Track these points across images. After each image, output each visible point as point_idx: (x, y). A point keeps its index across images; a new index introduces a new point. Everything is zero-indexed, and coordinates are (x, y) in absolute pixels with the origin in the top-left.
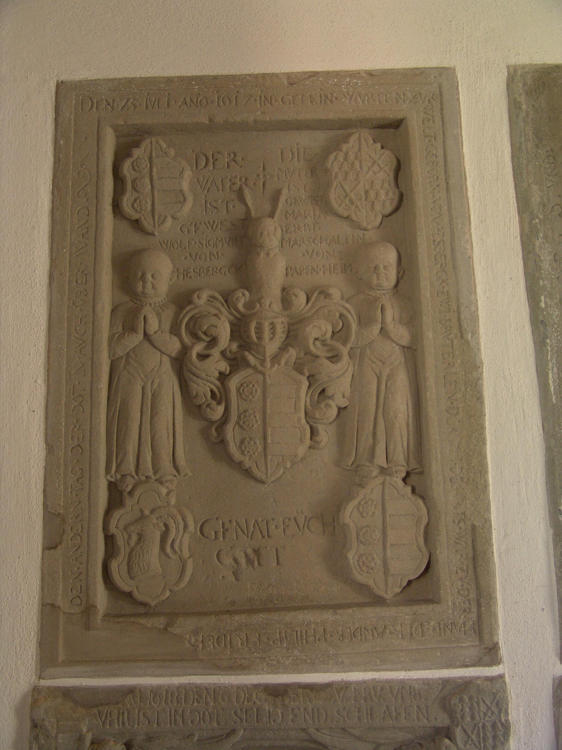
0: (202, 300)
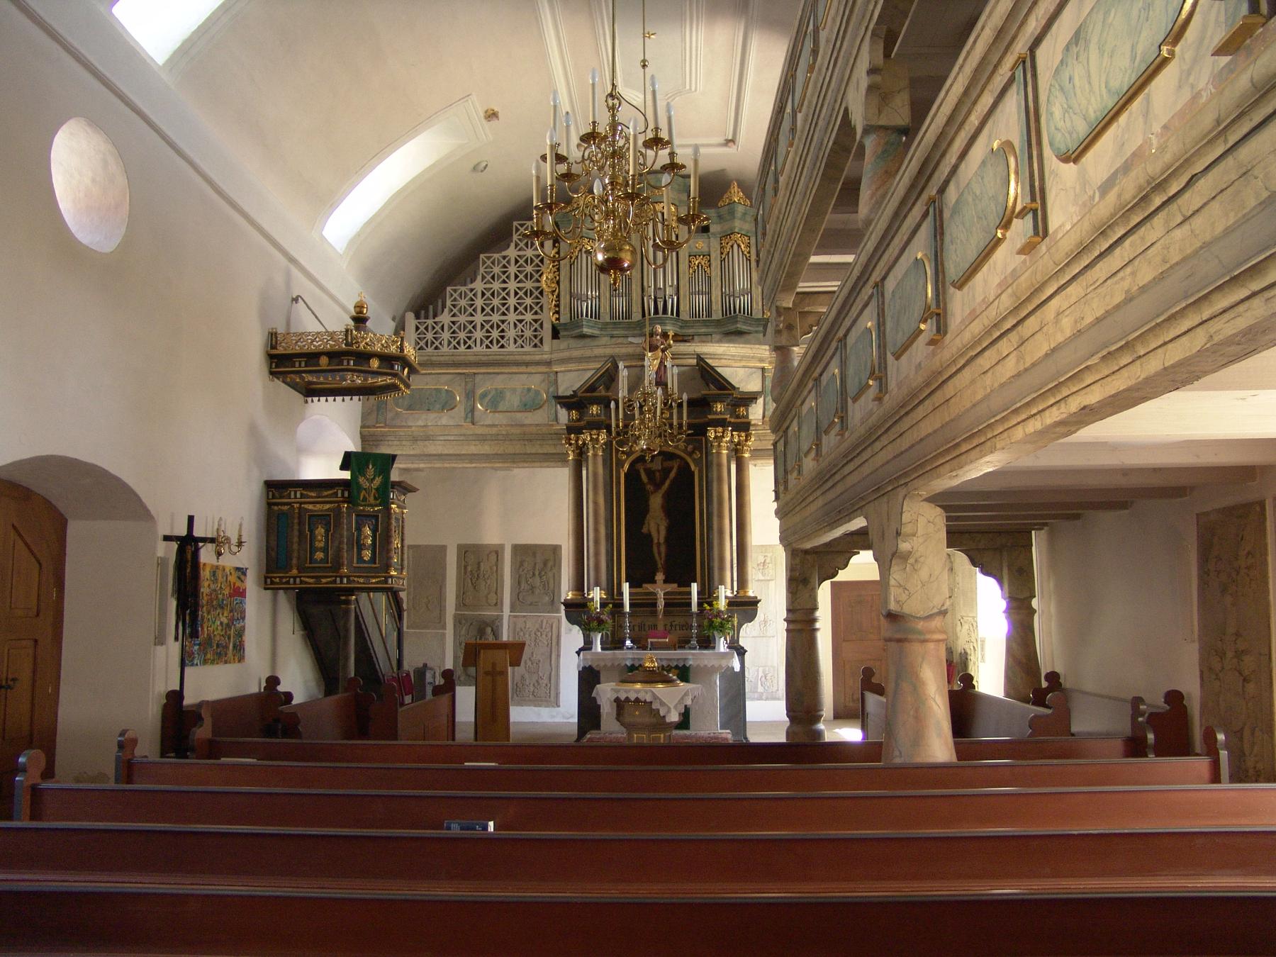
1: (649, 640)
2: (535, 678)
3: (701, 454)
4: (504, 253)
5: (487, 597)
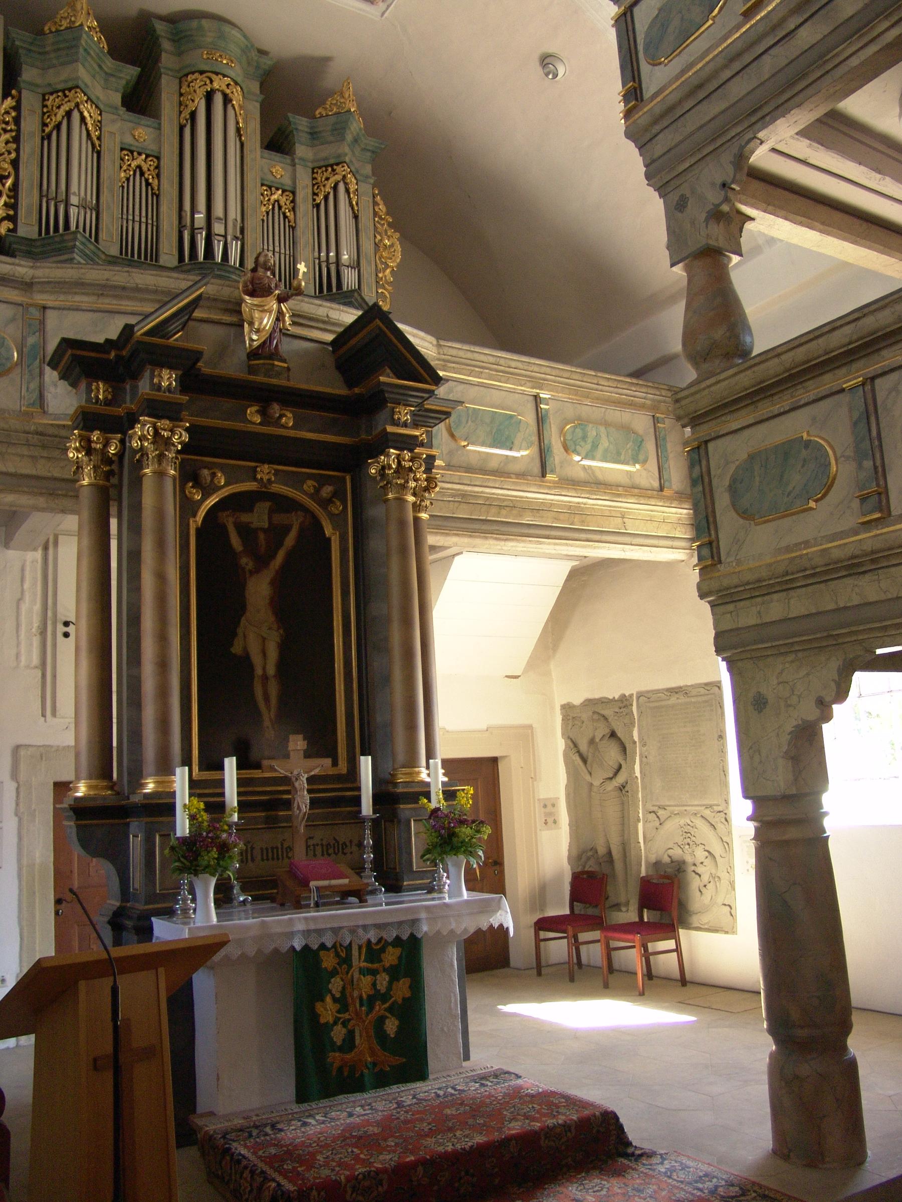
3: (344, 503)
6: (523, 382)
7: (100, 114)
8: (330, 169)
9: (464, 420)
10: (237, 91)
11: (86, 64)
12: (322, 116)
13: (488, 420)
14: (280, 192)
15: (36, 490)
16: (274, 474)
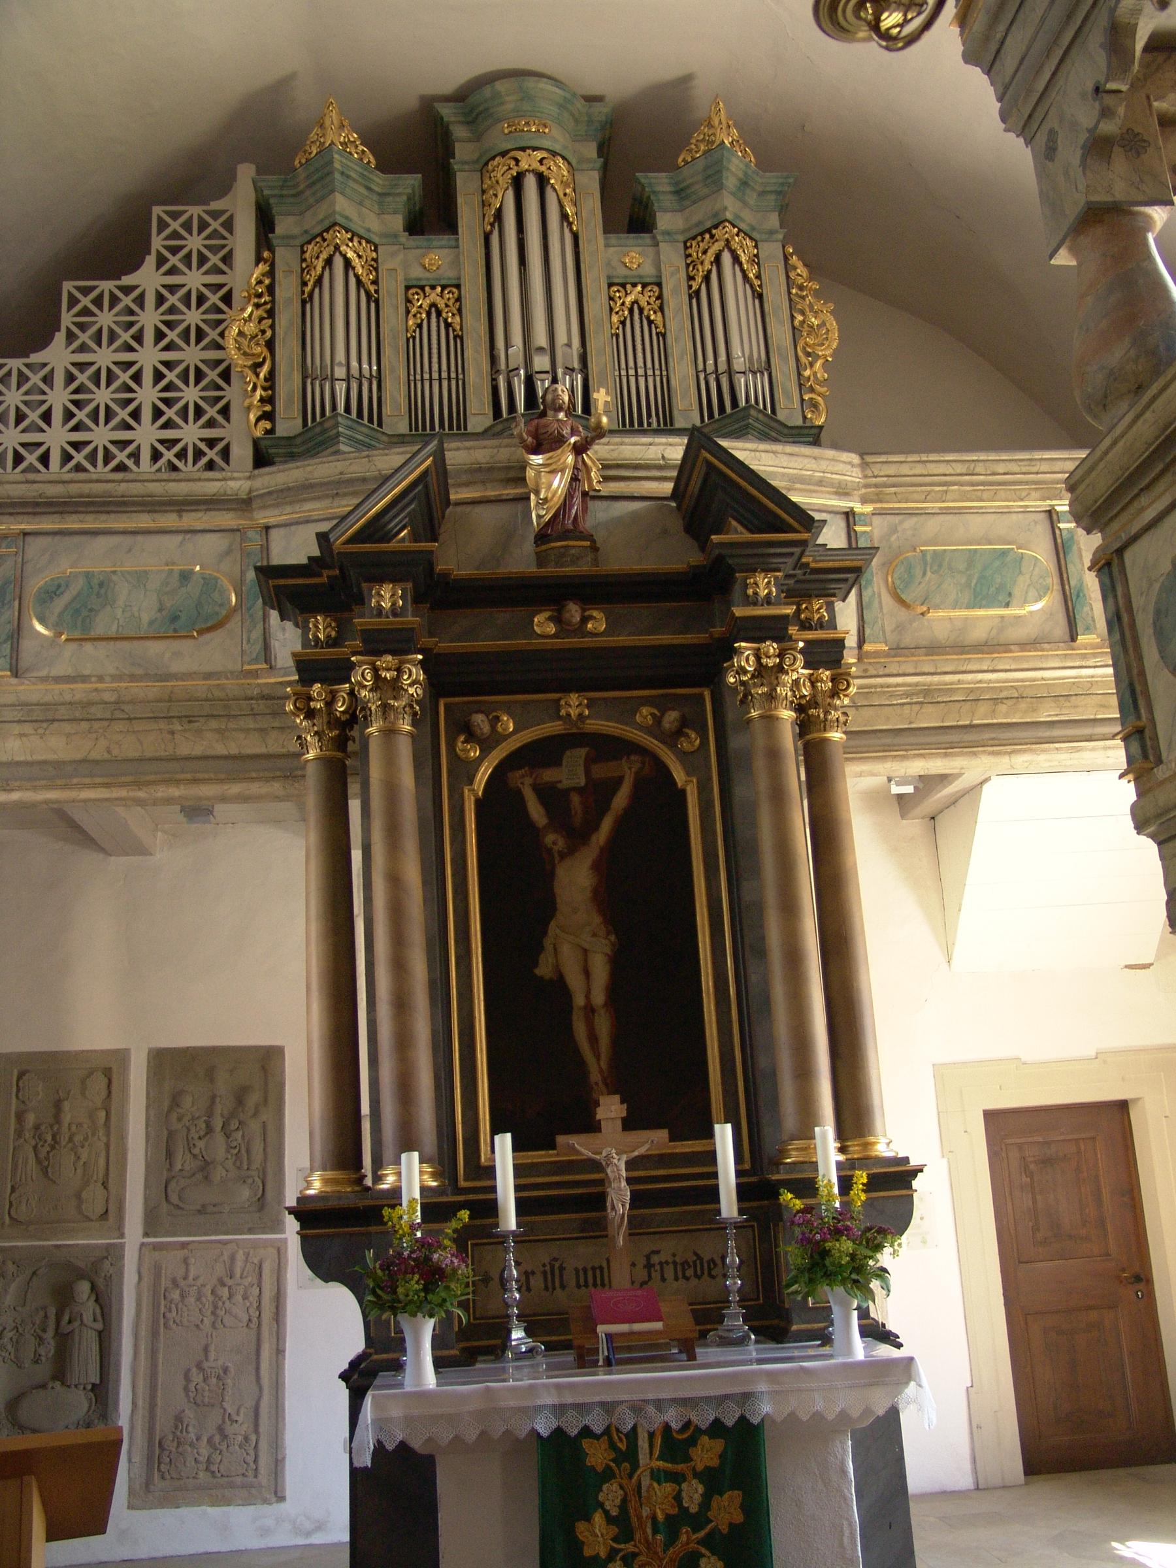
0: (43, 1127)
1: (602, 1329)
2: (214, 1418)
4: (126, 280)
5: (78, 1196)
6: (1024, 494)
7: (376, 250)
8: (707, 236)
9: (918, 572)
10: (556, 165)
11: (348, 191)
12: (687, 163)
13: (962, 566)
14: (639, 288)
15: (267, 774)
16: (588, 706)
